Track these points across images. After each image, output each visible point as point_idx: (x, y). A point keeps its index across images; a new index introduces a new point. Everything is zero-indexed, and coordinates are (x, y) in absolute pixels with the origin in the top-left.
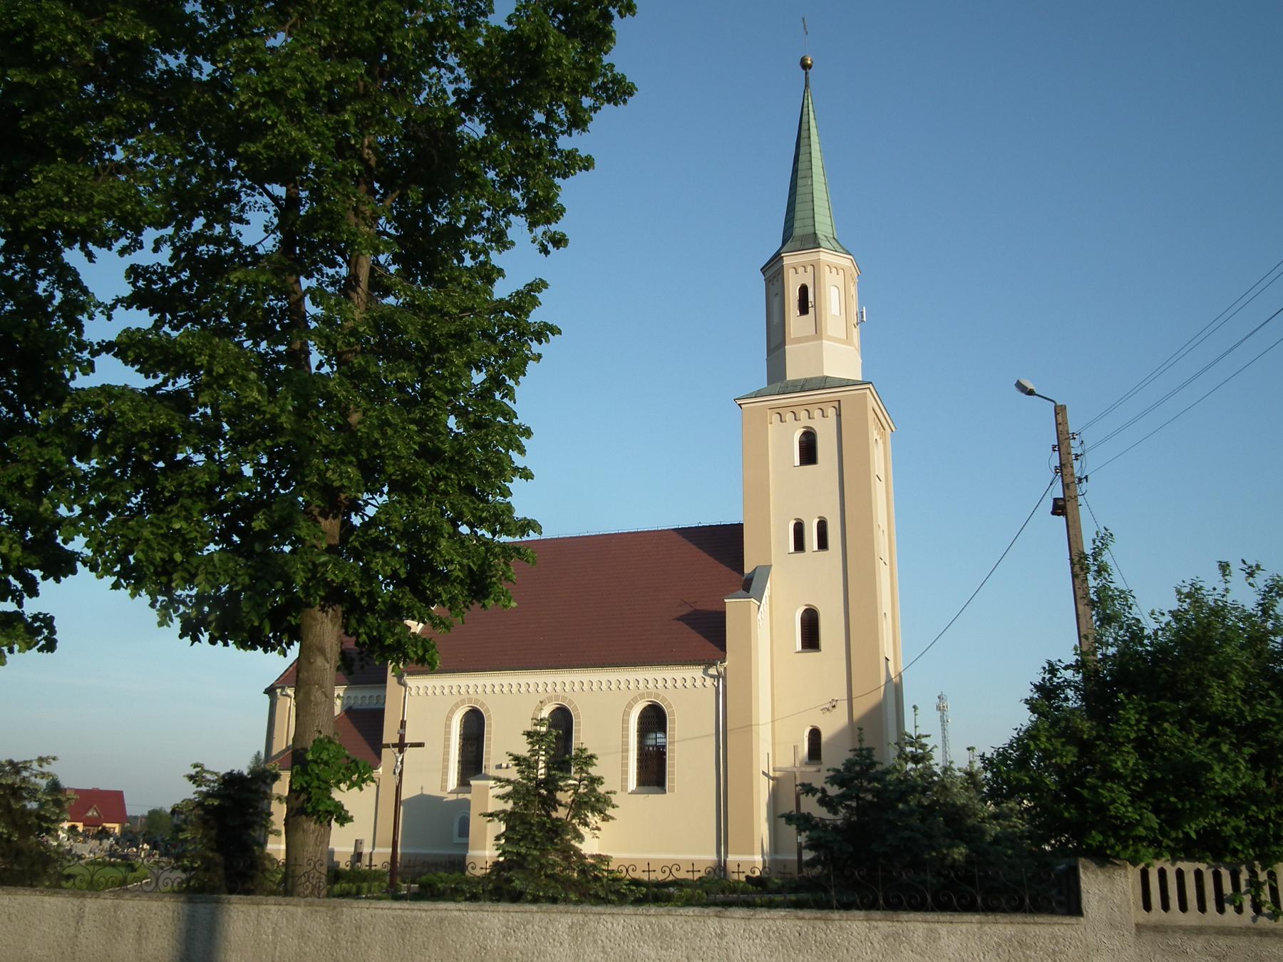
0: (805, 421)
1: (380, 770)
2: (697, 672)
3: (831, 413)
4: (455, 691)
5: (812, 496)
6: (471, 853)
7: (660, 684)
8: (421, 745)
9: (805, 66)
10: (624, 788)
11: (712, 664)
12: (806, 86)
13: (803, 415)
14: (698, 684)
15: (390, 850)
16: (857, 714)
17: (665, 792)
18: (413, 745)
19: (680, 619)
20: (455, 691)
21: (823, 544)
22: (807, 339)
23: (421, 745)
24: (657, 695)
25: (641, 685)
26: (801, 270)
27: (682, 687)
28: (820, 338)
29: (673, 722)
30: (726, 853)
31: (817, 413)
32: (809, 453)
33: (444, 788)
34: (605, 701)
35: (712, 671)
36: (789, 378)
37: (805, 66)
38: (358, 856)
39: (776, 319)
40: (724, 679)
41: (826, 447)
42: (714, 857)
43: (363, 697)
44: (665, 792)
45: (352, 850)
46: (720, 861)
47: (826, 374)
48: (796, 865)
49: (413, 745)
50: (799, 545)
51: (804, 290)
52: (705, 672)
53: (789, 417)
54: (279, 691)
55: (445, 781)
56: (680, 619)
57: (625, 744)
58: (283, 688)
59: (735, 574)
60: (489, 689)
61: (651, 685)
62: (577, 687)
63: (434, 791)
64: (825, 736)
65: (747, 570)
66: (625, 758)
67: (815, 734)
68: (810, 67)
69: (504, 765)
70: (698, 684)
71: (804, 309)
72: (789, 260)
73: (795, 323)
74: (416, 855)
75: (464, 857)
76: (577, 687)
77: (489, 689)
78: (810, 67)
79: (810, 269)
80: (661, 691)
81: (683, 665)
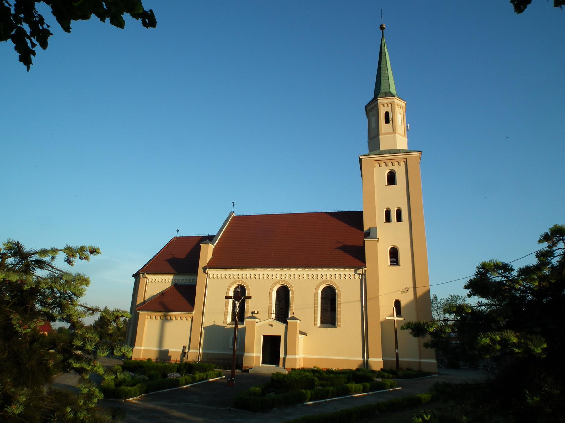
0: (390, 167)
1: (194, 313)
2: (351, 272)
3: (403, 164)
4: (232, 277)
5: (395, 197)
6: (246, 354)
7: (333, 277)
9: (382, 28)
10: (315, 325)
11: (359, 268)
13: (390, 164)
14: (352, 277)
16: (418, 294)
17: (336, 327)
19: (338, 248)
20: (232, 277)
21: (399, 219)
24: (332, 282)
25: (324, 277)
26: (386, 105)
27: (344, 279)
28: (395, 133)
29: (340, 294)
30: (368, 357)
31: (396, 164)
32: (392, 179)
33: (225, 322)
34: (306, 283)
35: (360, 271)
37: (382, 28)
38: (184, 354)
39: (373, 125)
40: (365, 275)
42: (361, 359)
43: (184, 279)
44: (336, 327)
45: (182, 350)
46: (364, 361)
47: (398, 148)
48: (395, 363)
50: (388, 219)
51: (387, 114)
52: (355, 272)
53: (383, 165)
54: (141, 275)
55: (226, 318)
56: (338, 248)
57: (316, 304)
58: (144, 274)
59: (360, 231)
60: (248, 277)
62: (292, 277)
63: (220, 323)
64: (403, 304)
65: (366, 229)
66: (316, 310)
67: (397, 304)
68: (384, 28)
69: (256, 312)
70: (352, 277)
71: (387, 121)
72: (380, 101)
73: (383, 127)
74: (213, 354)
76: (292, 277)
77: (248, 277)
78: (384, 28)
79: (390, 105)
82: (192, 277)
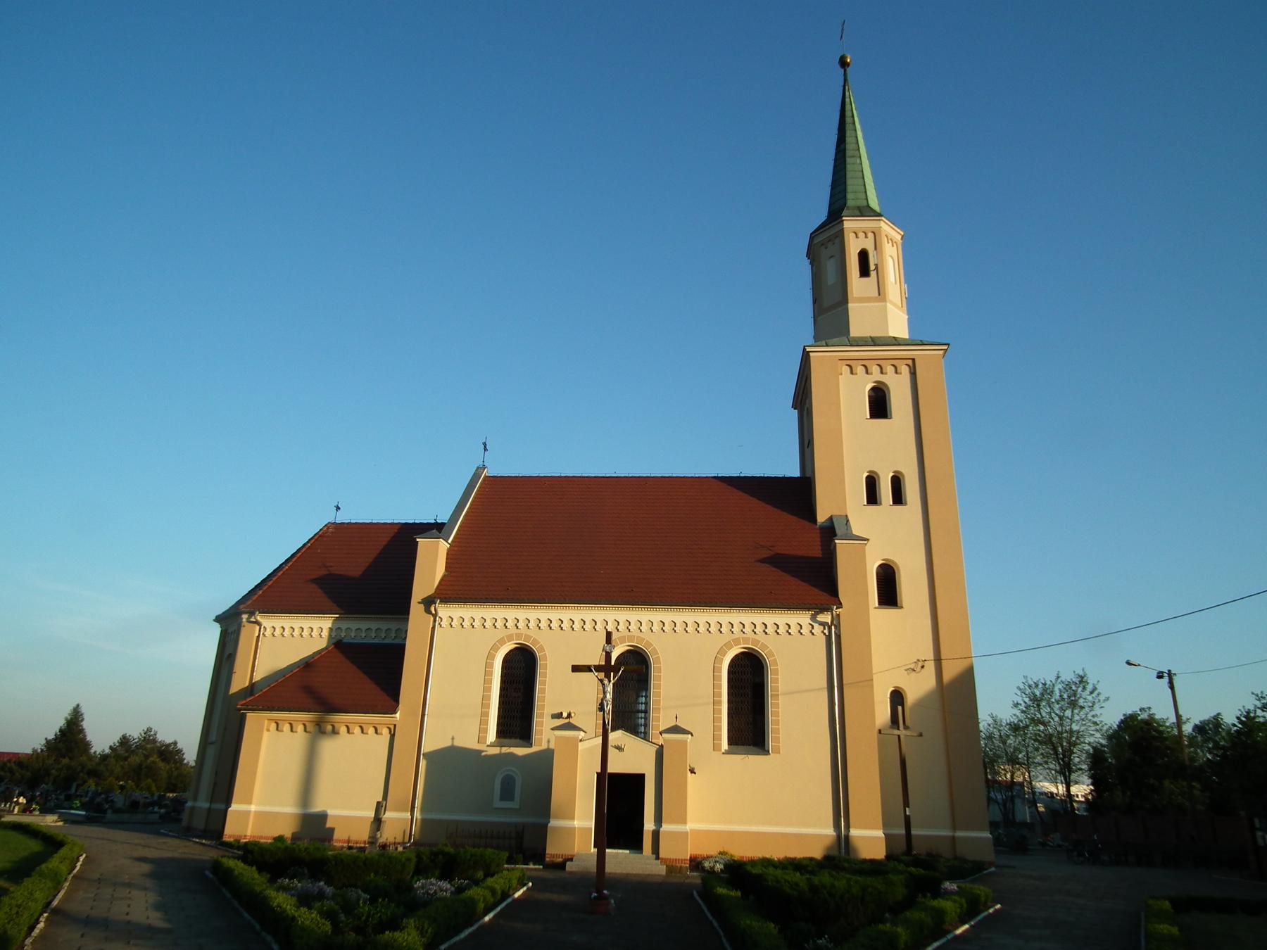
0: (876, 376)
1: (398, 715)
2: (804, 618)
3: (905, 371)
4: (499, 624)
5: (888, 447)
6: (553, 823)
7: (759, 629)
8: (576, 669)
9: (843, 63)
10: (716, 747)
11: (823, 609)
12: (845, 81)
13: (875, 369)
14: (805, 631)
15: (903, 832)
16: (948, 675)
17: (767, 753)
18: (587, 669)
19: (763, 561)
20: (499, 624)
21: (898, 498)
22: (869, 300)
23: (576, 669)
24: (756, 642)
25: (736, 629)
26: (861, 235)
28: (884, 300)
29: (776, 672)
30: (848, 827)
31: (890, 369)
32: (879, 405)
33: (481, 739)
34: (691, 646)
35: (826, 617)
36: (852, 334)
37: (843, 63)
38: (378, 822)
39: (831, 277)
40: (838, 627)
41: (900, 400)
42: (830, 831)
43: (365, 629)
44: (767, 753)
45: (372, 814)
46: (839, 836)
47: (892, 334)
48: (904, 840)
49: (587, 669)
50: (873, 498)
51: (863, 256)
52: (813, 618)
53: (860, 370)
54: (245, 617)
55: (483, 731)
56: (763, 561)
57: (717, 695)
58: (252, 614)
59: (806, 523)
60: (544, 625)
61: (748, 629)
62: (656, 628)
63: (470, 742)
64: (911, 697)
65: (821, 518)
66: (717, 712)
67: (897, 697)
68: (848, 65)
69: (565, 715)
70: (805, 631)
71: (864, 272)
72: (849, 224)
73: (857, 285)
74: (457, 822)
75: (546, 826)
76: (656, 628)
77: (544, 625)
78: (848, 65)
79: (870, 235)
80: (760, 636)
81: (789, 608)
82: (394, 626)
